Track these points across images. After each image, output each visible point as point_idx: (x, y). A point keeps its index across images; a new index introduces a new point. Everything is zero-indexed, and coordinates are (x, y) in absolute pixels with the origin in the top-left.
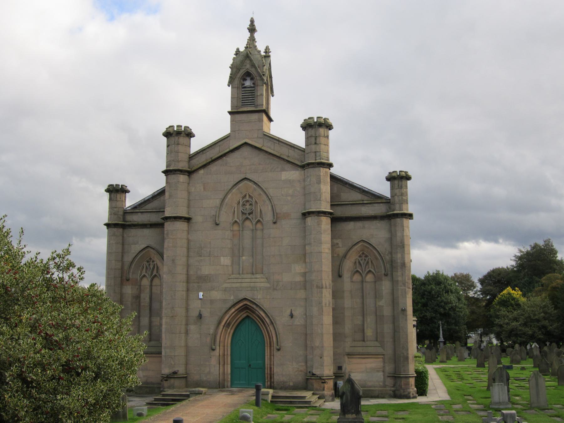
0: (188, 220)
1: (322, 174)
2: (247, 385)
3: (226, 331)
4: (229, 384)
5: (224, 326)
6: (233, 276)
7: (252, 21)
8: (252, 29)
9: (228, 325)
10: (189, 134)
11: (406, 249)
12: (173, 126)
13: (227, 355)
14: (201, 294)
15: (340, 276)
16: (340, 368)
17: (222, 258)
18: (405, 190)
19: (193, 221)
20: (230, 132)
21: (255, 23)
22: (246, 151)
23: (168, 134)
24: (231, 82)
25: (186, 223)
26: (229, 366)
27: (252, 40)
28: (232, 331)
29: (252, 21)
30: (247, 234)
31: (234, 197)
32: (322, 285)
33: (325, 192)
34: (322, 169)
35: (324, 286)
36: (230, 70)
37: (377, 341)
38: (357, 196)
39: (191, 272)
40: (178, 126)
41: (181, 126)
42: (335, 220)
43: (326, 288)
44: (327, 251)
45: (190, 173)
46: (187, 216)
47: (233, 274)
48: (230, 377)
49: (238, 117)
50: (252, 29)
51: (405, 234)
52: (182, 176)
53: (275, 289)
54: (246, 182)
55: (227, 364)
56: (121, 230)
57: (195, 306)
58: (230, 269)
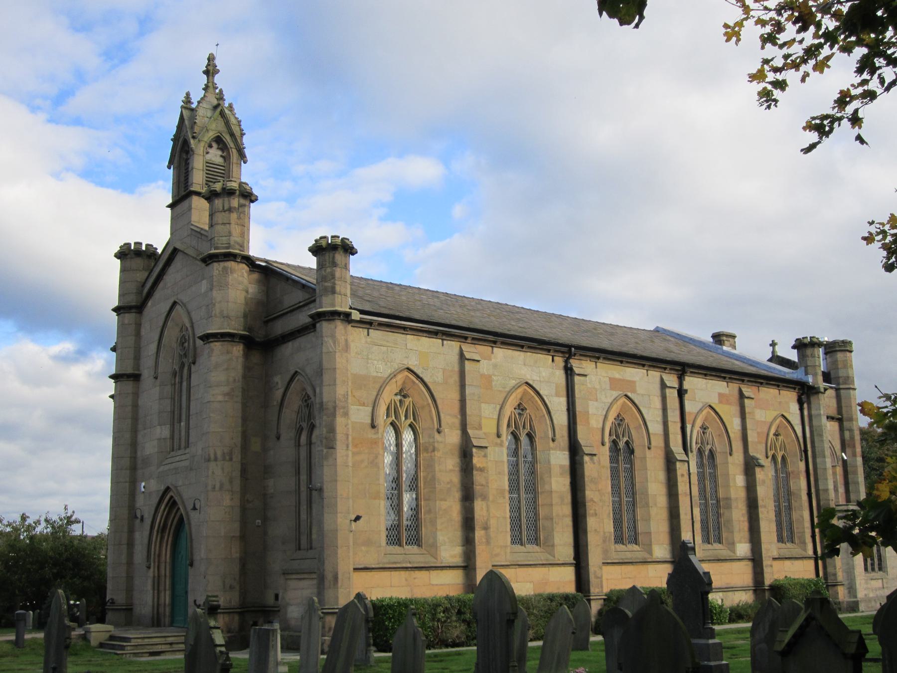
1: (216, 273)
2: (883, 653)
3: (162, 538)
4: (167, 620)
5: (158, 532)
6: (172, 454)
7: (211, 59)
8: (210, 71)
9: (163, 529)
11: (326, 378)
12: (129, 245)
13: (165, 575)
14: (143, 484)
15: (278, 438)
16: (277, 597)
17: (158, 429)
18: (329, 270)
19: (142, 378)
20: (169, 236)
21: (217, 62)
24: (171, 162)
25: (131, 383)
26: (168, 593)
28: (170, 539)
29: (211, 59)
31: (172, 335)
32: (209, 455)
33: (220, 302)
34: (215, 264)
35: (212, 456)
36: (172, 143)
37: (300, 549)
39: (139, 454)
40: (136, 243)
41: (141, 244)
43: (216, 459)
44: (220, 398)
46: (130, 371)
47: (173, 450)
48: (168, 610)
49: (179, 208)
50: (210, 71)
51: (324, 350)
52: (127, 315)
53: (191, 469)
55: (165, 590)
58: (168, 443)
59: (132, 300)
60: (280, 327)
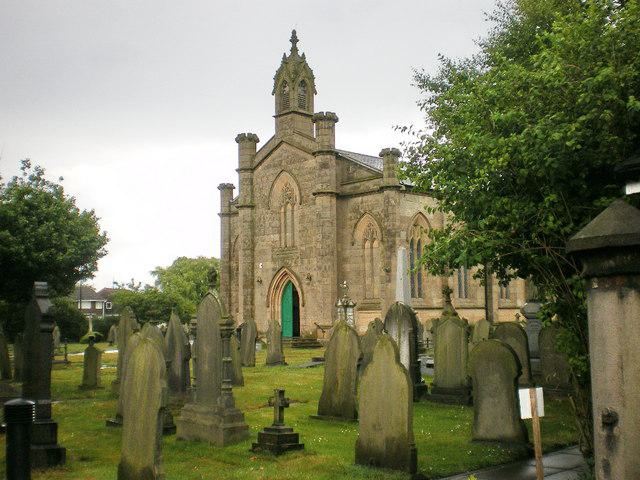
0: (252, 207)
7: (294, 32)
8: (294, 40)
10: (253, 139)
22: (284, 146)
23: (241, 139)
27: (294, 50)
29: (294, 32)
30: (289, 214)
38: (365, 174)
42: (341, 197)
45: (253, 170)
50: (294, 40)
54: (284, 173)
56: (227, 218)
57: (258, 274)
59: (247, 165)
60: (348, 189)
